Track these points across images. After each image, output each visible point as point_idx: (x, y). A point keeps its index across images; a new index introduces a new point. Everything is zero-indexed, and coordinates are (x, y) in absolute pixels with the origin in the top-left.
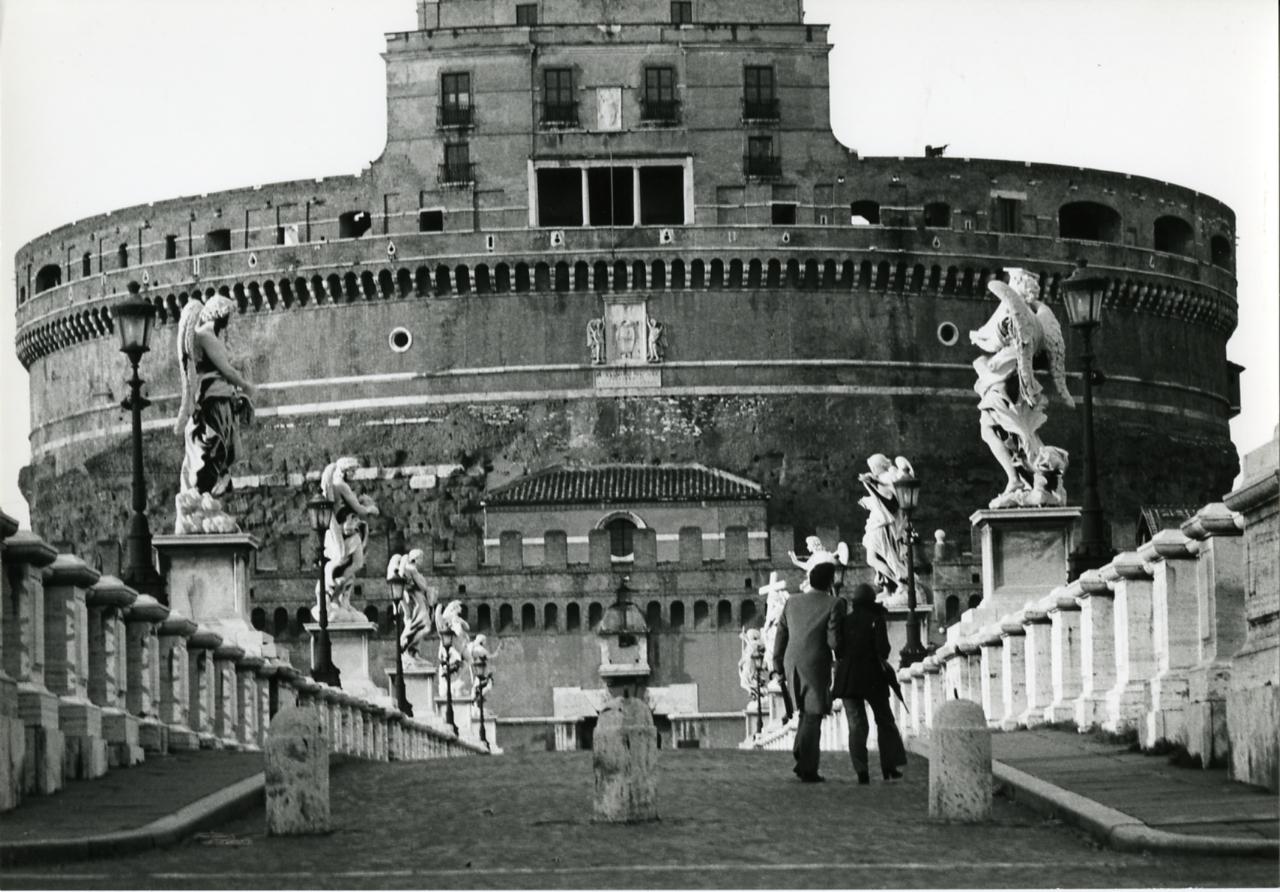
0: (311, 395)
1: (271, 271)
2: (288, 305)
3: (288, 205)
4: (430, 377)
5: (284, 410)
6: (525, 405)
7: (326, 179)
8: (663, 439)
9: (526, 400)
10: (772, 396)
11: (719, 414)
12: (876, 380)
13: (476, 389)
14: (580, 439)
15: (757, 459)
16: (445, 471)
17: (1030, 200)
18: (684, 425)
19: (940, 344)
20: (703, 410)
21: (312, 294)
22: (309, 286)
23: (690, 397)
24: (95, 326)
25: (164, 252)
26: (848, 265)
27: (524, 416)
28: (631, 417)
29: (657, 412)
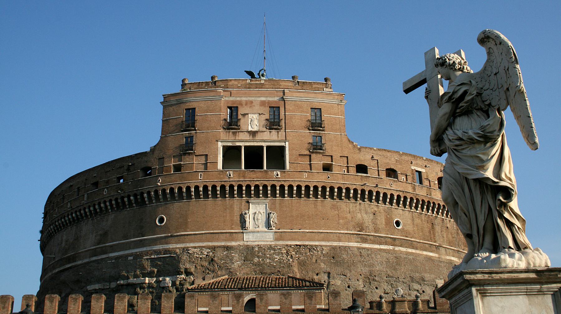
3: (121, 167)
4: (171, 236)
6: (214, 248)
7: (136, 155)
8: (275, 264)
9: (212, 246)
11: (301, 253)
12: (369, 242)
13: (192, 241)
14: (237, 264)
15: (317, 274)
17: (426, 172)
20: (293, 252)
21: (127, 203)
22: (126, 199)
23: (287, 245)
24: (53, 230)
26: (355, 190)
27: (213, 253)
29: (272, 252)
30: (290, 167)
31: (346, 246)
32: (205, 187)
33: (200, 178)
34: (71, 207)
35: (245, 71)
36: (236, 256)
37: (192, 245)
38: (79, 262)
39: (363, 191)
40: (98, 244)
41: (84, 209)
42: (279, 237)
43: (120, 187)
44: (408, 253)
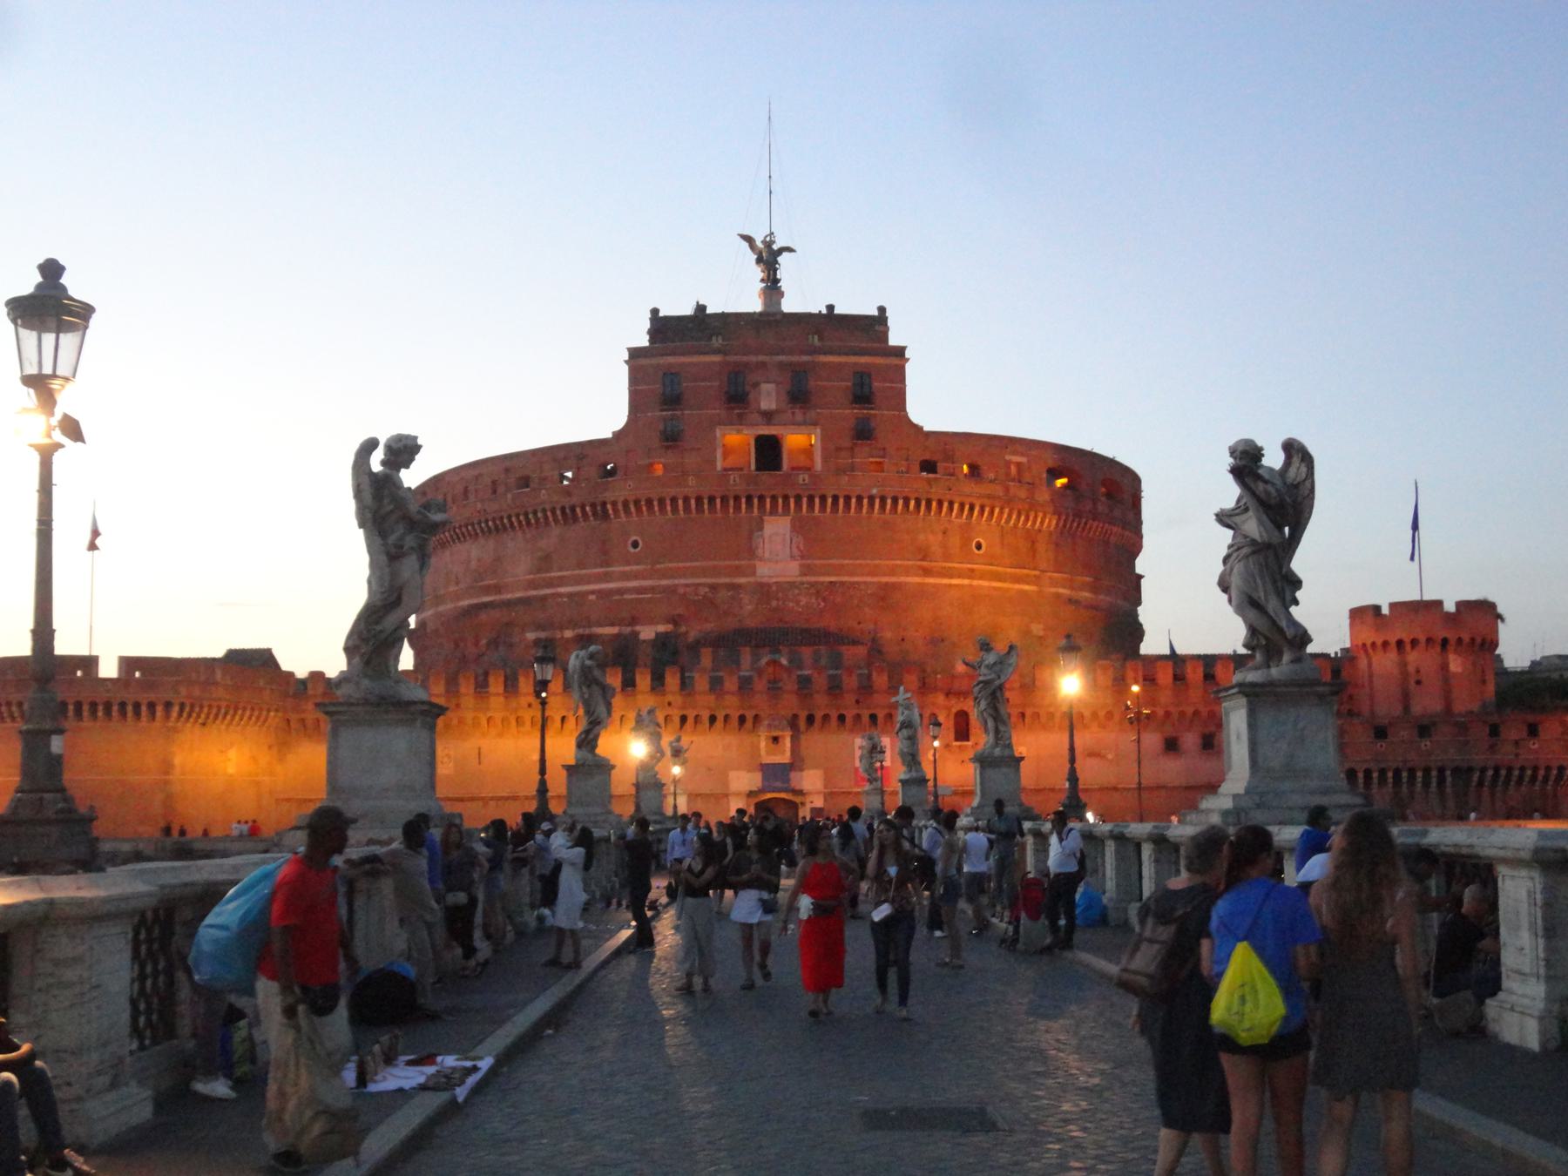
0: (579, 580)
1: (555, 498)
2: (565, 524)
5: (562, 590)
6: (713, 587)
10: (871, 583)
15: (859, 623)
16: (661, 628)
17: (1028, 461)
18: (813, 600)
19: (974, 553)
22: (578, 510)
23: (816, 583)
24: (449, 539)
25: (490, 491)
28: (780, 595)
29: (797, 591)
30: (823, 466)
31: (900, 583)
32: (699, 500)
33: (690, 484)
34: (485, 510)
35: (739, 235)
36: (746, 598)
37: (683, 581)
38: (509, 596)
39: (929, 502)
40: (539, 571)
41: (509, 517)
42: (807, 570)
43: (567, 492)
44: (989, 587)
